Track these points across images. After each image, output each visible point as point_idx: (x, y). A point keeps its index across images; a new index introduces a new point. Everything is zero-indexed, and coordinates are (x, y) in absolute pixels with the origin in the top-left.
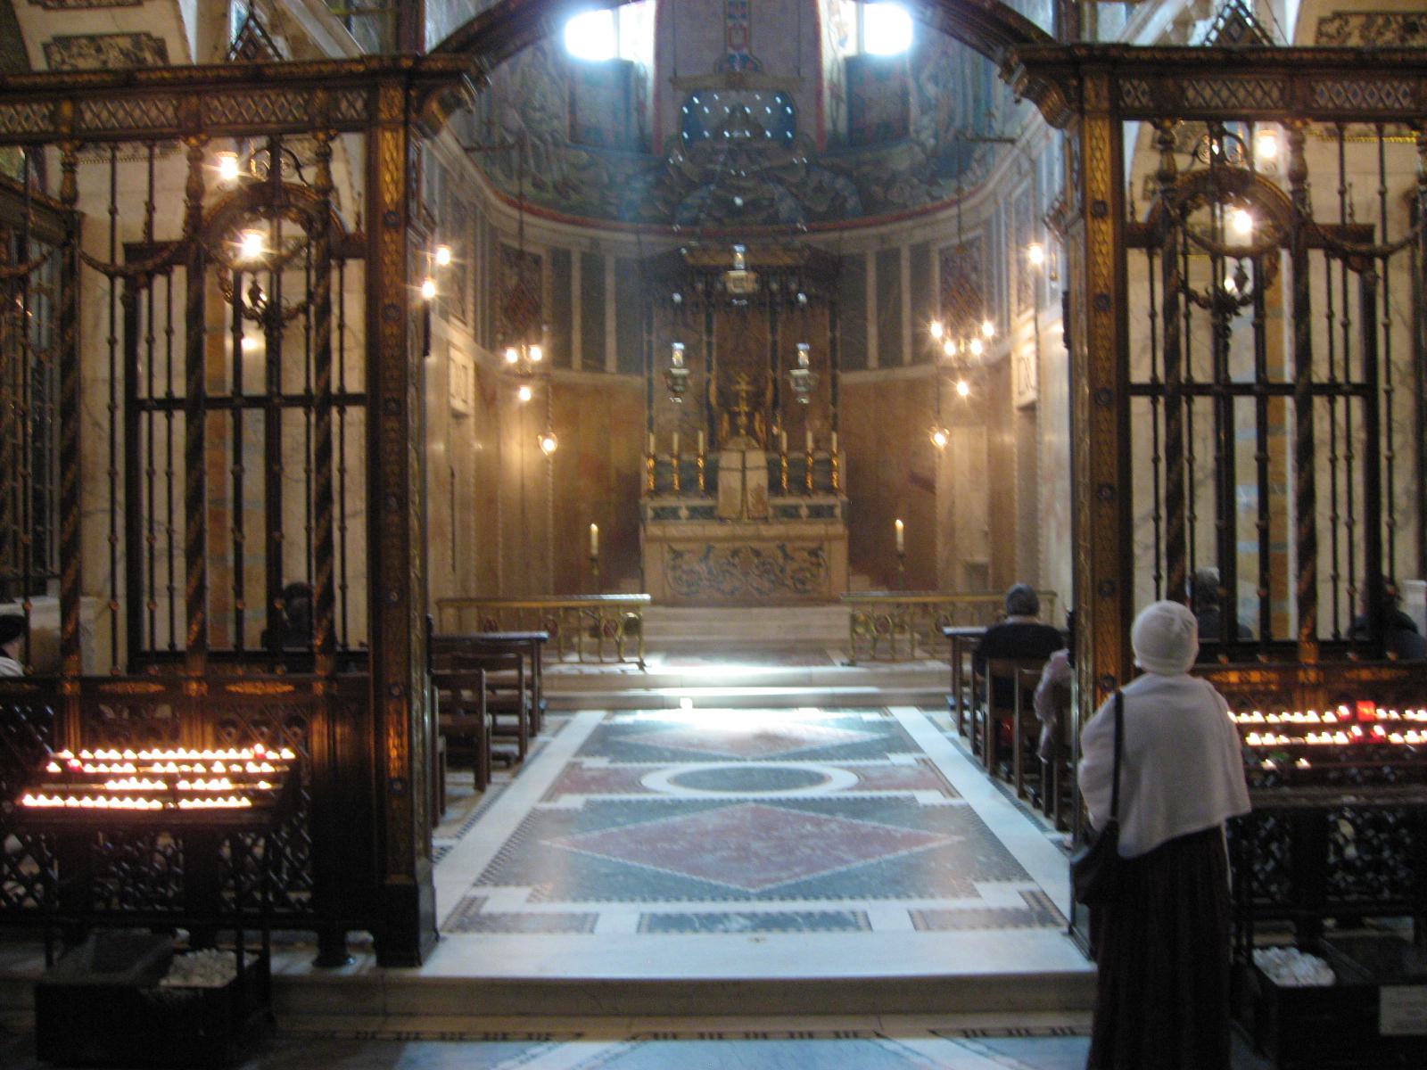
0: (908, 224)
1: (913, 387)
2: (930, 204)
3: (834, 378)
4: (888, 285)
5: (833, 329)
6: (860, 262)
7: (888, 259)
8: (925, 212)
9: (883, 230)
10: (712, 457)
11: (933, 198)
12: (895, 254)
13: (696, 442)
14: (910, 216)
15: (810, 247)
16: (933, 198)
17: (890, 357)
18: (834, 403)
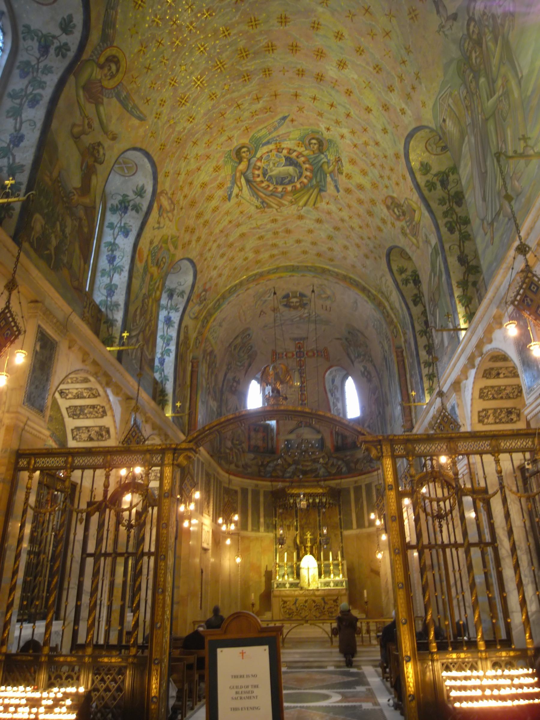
0: (364, 476)
1: (369, 536)
2: (370, 469)
3: (341, 533)
4: (358, 499)
5: (340, 514)
6: (348, 491)
7: (358, 489)
8: (369, 472)
9: (355, 479)
10: (298, 563)
11: (372, 468)
12: (360, 487)
13: (293, 557)
14: (364, 474)
15: (329, 486)
16: (372, 468)
17: (361, 525)
18: (342, 542)
